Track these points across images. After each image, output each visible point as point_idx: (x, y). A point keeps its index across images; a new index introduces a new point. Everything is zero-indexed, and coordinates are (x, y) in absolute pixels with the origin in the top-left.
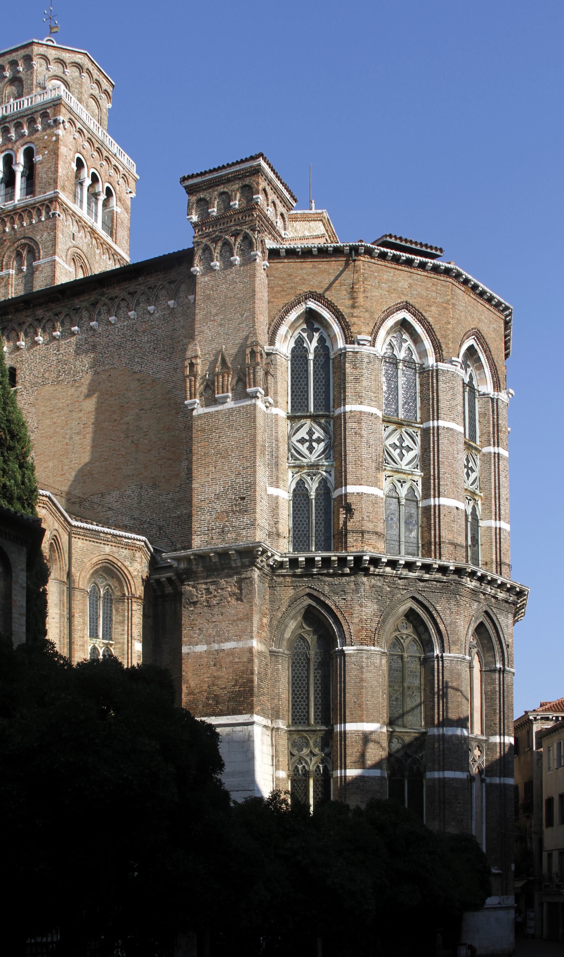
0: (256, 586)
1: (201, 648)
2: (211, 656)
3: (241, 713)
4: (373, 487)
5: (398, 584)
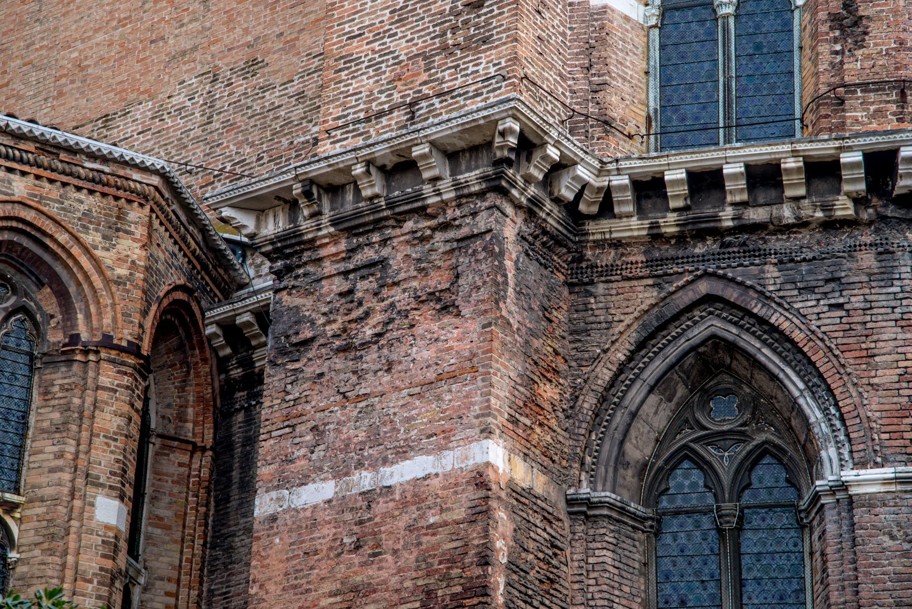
0: (508, 264)
2: (348, 516)
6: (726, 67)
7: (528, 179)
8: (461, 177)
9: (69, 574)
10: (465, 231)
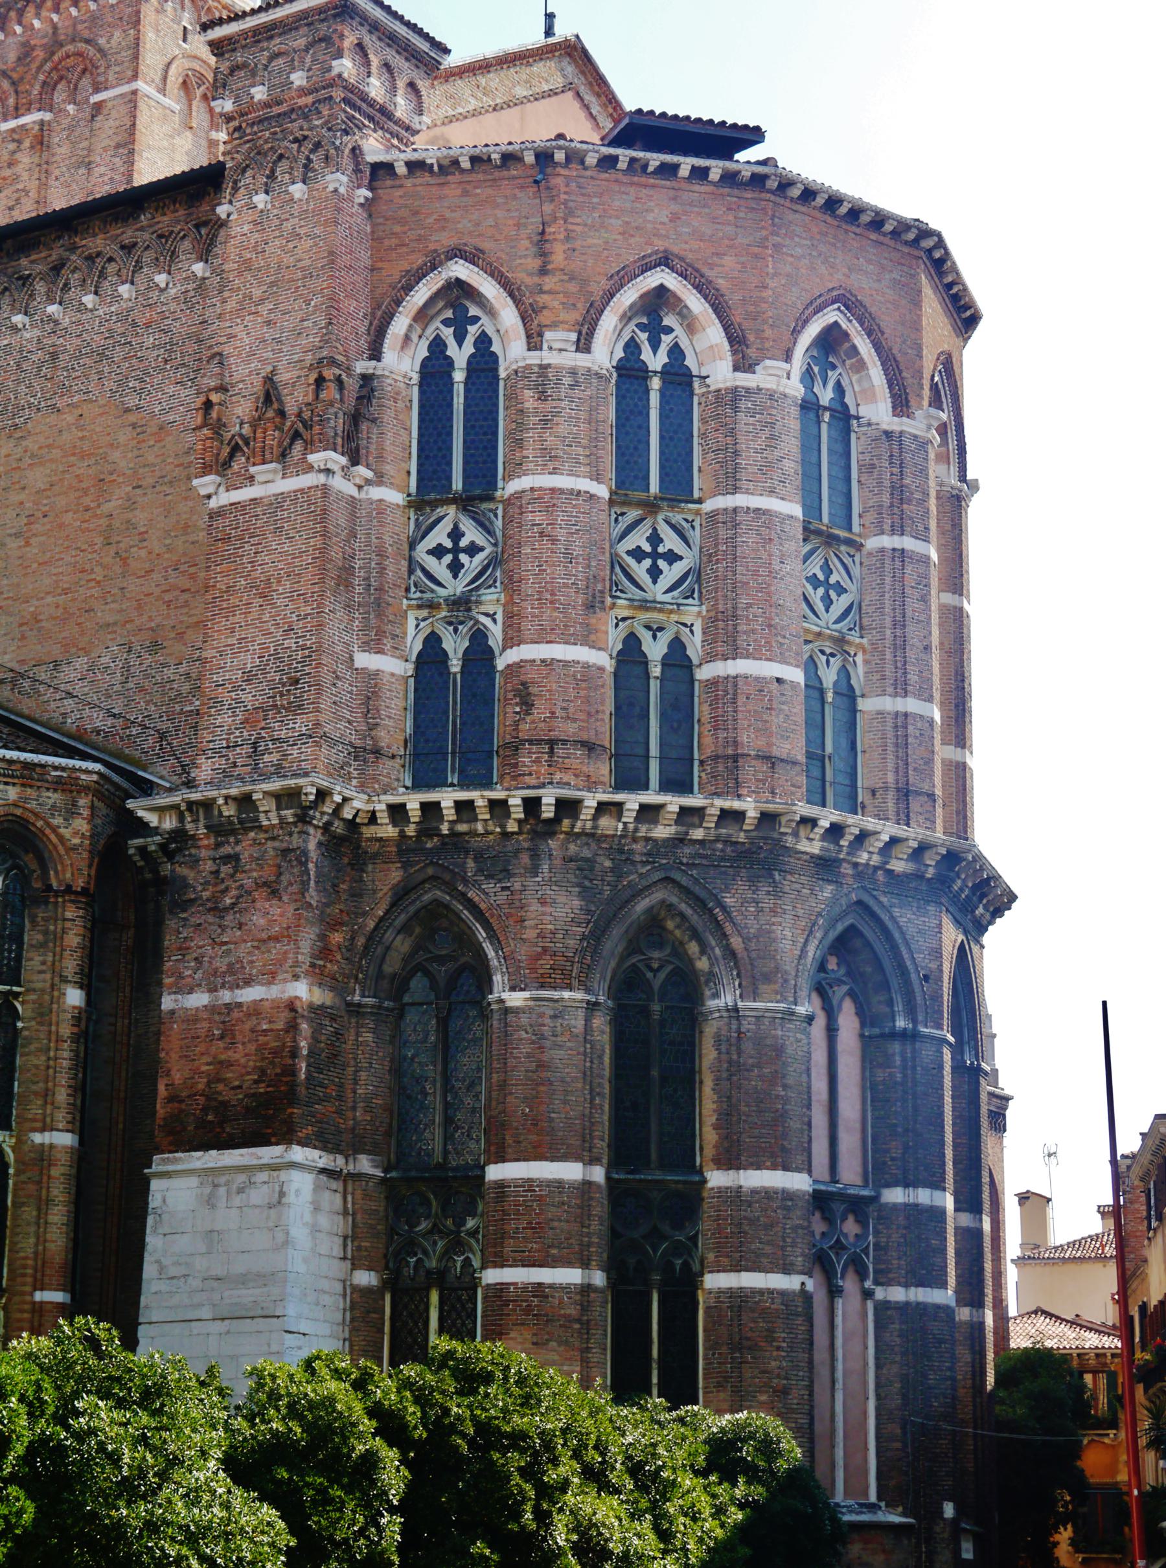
0: (311, 866)
1: (199, 1000)
2: (217, 1017)
3: (267, 1143)
4: (578, 647)
5: (631, 851)
6: (455, 709)
7: (323, 813)
8: (283, 813)
9: (53, 1038)
10: (285, 845)
